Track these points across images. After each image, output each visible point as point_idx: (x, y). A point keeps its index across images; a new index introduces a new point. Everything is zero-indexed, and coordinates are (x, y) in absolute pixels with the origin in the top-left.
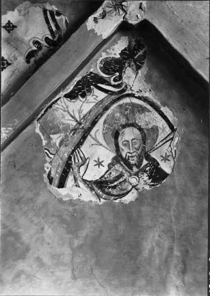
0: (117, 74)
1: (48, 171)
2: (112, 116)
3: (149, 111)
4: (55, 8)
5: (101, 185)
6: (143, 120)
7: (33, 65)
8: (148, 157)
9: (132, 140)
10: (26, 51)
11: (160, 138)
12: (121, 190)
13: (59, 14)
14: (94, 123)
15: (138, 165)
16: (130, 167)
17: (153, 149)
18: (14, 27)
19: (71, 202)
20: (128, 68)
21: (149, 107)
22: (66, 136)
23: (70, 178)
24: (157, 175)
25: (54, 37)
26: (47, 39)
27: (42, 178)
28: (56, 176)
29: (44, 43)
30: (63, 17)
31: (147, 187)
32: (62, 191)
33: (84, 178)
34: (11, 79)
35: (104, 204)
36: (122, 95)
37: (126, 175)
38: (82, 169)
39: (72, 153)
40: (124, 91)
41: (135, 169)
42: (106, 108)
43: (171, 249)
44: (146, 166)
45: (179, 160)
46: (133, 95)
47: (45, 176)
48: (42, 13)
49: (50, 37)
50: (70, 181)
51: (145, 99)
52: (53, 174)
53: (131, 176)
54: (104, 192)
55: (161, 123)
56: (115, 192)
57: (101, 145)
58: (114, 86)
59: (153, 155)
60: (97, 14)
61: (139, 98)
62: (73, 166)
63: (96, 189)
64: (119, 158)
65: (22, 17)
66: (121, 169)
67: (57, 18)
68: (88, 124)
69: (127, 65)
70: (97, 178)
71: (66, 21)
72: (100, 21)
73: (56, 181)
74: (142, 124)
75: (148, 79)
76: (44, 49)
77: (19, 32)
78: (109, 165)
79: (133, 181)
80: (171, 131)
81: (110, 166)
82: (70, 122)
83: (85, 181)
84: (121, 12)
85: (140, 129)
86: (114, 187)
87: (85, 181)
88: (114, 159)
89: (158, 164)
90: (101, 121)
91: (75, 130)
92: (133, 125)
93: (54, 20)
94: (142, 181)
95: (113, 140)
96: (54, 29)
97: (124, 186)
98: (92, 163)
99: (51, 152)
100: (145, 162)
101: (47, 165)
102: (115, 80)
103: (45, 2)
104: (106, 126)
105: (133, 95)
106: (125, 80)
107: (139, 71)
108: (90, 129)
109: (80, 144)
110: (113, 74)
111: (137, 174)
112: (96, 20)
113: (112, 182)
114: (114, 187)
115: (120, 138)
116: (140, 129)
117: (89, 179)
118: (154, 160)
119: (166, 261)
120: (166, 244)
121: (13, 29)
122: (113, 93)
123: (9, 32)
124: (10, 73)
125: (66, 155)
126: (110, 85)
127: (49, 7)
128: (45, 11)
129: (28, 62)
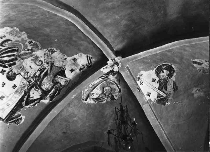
0: (107, 75)
1: (82, 98)
2: (103, 84)
3: (114, 85)
4: (91, 56)
5: (97, 99)
6: (112, 86)
7: (81, 72)
8: (111, 94)
9: (108, 90)
10: (80, 67)
11: (116, 91)
12: (102, 100)
13: (92, 58)
14: (97, 85)
15: (108, 95)
17: (113, 93)
18: (77, 60)
19: (88, 104)
20: (111, 75)
21: (115, 84)
22: (89, 89)
23: (89, 99)
24: (113, 98)
26: (87, 65)
27: (81, 100)
28: (85, 98)
29: (86, 66)
30: (93, 59)
31: (109, 101)
32: (86, 102)
33: (93, 98)
34: (74, 75)
35: (97, 103)
36: (108, 79)
37: (104, 97)
38: (92, 96)
39: (90, 92)
40: (108, 79)
41: (107, 96)
42: (102, 82)
43: (112, 115)
44: (110, 96)
45: (120, 98)
46: (111, 80)
47: (82, 99)
48: (86, 57)
49: (88, 65)
50: (88, 99)
51: (114, 82)
52: (84, 98)
54: (97, 101)
55: (117, 89)
57: (99, 90)
58: (106, 78)
59: (113, 94)
60: (105, 67)
61: (112, 81)
62: (90, 95)
64: (103, 93)
65: (79, 57)
66: (103, 96)
67: (91, 59)
68: (96, 86)
69: (111, 74)
70: (96, 97)
71: (94, 61)
72: (105, 69)
73: (85, 100)
74: (112, 87)
75: (116, 78)
76: (86, 68)
77: (78, 62)
78: (100, 94)
79: (106, 98)
80: (119, 90)
83: (92, 99)
84: (112, 68)
85: (111, 88)
86: (100, 100)
87: (92, 99)
88: (102, 93)
89: (114, 97)
91: (92, 87)
92: (109, 86)
94: (108, 99)
95: (102, 89)
96: (90, 62)
98: (95, 95)
100: (110, 95)
101: (83, 96)
102: (106, 76)
103: (88, 54)
104: (101, 86)
105: (111, 80)
106: (109, 77)
107: (114, 76)
108: (96, 87)
109: (93, 90)
110: (105, 75)
111: (107, 97)
112: (104, 69)
114: (100, 100)
115: (104, 89)
116: (111, 88)
118: (113, 95)
119: (110, 117)
120: (111, 113)
121: (76, 61)
122: (105, 79)
123: (75, 61)
124: (74, 74)
125: (88, 93)
126: (104, 77)
127: (89, 56)
128: (87, 56)
129: (80, 71)
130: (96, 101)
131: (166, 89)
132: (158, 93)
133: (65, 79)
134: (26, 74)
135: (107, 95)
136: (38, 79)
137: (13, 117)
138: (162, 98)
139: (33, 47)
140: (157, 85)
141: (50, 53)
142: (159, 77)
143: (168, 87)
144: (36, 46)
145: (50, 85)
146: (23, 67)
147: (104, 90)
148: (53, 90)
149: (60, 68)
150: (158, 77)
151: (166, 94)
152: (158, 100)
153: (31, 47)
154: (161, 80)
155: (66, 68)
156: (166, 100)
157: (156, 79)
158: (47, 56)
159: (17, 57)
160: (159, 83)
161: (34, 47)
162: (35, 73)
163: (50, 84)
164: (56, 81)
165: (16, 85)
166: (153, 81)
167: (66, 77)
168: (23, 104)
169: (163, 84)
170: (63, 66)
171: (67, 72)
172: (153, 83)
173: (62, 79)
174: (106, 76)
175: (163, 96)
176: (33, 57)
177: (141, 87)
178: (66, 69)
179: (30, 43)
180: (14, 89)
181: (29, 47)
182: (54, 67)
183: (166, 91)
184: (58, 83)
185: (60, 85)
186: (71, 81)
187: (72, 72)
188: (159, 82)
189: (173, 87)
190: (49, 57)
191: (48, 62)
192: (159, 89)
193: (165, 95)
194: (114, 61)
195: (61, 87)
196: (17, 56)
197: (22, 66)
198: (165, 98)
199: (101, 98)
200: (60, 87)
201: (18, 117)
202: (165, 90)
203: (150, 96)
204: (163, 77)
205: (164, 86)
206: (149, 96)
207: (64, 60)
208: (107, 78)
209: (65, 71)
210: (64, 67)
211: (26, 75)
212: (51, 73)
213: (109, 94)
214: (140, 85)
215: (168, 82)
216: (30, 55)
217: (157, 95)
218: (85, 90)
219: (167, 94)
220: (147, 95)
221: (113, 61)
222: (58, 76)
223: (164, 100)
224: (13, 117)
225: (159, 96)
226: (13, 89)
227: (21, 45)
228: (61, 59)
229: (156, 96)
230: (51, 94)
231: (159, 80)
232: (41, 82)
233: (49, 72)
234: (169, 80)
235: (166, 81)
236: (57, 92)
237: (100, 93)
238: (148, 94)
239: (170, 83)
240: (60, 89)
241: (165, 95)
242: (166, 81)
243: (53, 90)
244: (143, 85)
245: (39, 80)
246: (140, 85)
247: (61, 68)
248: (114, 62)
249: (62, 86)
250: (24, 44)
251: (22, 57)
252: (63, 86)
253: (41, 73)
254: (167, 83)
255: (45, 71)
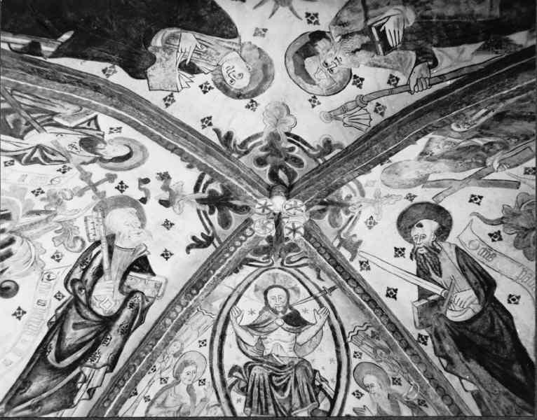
0: (265, 256)
5: (253, 327)
8: (291, 308)
16: (276, 312)
23: (230, 327)
25: (209, 232)
26: (202, 234)
38: (239, 319)
39: (230, 310)
40: (271, 265)
41: (281, 315)
49: (206, 233)
53: (277, 318)
56: (266, 330)
59: (295, 307)
63: (250, 330)
67: (209, 216)
80: (309, 295)
81: (261, 313)
82: (227, 291)
83: (240, 326)
87: (240, 326)
88: (264, 308)
90: (253, 286)
93: (208, 219)
97: (274, 326)
98: (246, 314)
99: (213, 313)
102: (263, 259)
113: (262, 323)
117: (244, 324)
122: (261, 267)
128: (198, 211)
129: (189, 253)
130: (254, 332)
131: (440, 273)
132: (418, 286)
133: (153, 278)
134: (46, 276)
135: (282, 312)
136: (80, 289)
137: (24, 395)
138: (432, 298)
139: (48, 203)
140: (412, 266)
141: (100, 216)
142: (411, 241)
143: (443, 265)
144: (54, 201)
145: (116, 301)
146: (33, 260)
147: (269, 298)
148: (127, 312)
149: (135, 250)
150: (410, 242)
151: (442, 286)
152: (423, 305)
153: (45, 203)
154: (418, 248)
155: (148, 250)
156: (445, 304)
157: (403, 249)
158: (93, 223)
159: (13, 235)
160: (416, 258)
161: (50, 205)
162: (71, 272)
163: (115, 298)
164: (129, 287)
165: (24, 308)
166: (396, 256)
167: (154, 275)
168: (48, 357)
169: (429, 259)
170: (140, 245)
171: (155, 261)
172: (397, 258)
173: (145, 279)
174: (263, 259)
175: (433, 294)
176: (56, 232)
177: (364, 274)
178: (149, 253)
179: (37, 195)
180: (19, 318)
181: (40, 206)
182: (115, 250)
183: (441, 276)
184: (134, 292)
185: (142, 299)
186: (169, 284)
187: (167, 259)
188: (414, 255)
189: (457, 265)
190: (97, 225)
191: (97, 238)
192: (418, 275)
193: (438, 290)
194: (267, 211)
195: (146, 304)
196: (11, 232)
197: (31, 257)
198: (442, 299)
199: (266, 321)
200: (143, 303)
201: (40, 395)
202: (437, 274)
203: (396, 298)
204: (426, 240)
205: (431, 266)
206: (395, 297)
207: (141, 230)
208: (267, 262)
209: (149, 257)
210: (144, 248)
211: (45, 280)
212: (113, 267)
213: (285, 308)
214: (362, 269)
215: (443, 253)
216: (46, 227)
217: (417, 294)
218: (213, 304)
219: (445, 286)
220: (388, 295)
221: (263, 211)
222: (132, 273)
223: (441, 302)
224: (27, 396)
225: (423, 294)
226: (18, 320)
227: (14, 202)
228: (131, 228)
229: (415, 295)
230: (121, 325)
231: (413, 250)
232: (89, 294)
233: (106, 266)
234: (443, 244)
235: (434, 251)
236: (138, 317)
237: (260, 309)
238: (389, 292)
239: (447, 254)
240: (145, 310)
241: (441, 289)
242: (434, 251)
243: (127, 312)
244: (369, 268)
245: (84, 291)
246: (362, 269)
247: (137, 251)
248: (268, 214)
249: (147, 301)
250: (22, 197)
251: (27, 233)
252: (150, 300)
253: (85, 271)
254: (439, 256)
255: (96, 263)
